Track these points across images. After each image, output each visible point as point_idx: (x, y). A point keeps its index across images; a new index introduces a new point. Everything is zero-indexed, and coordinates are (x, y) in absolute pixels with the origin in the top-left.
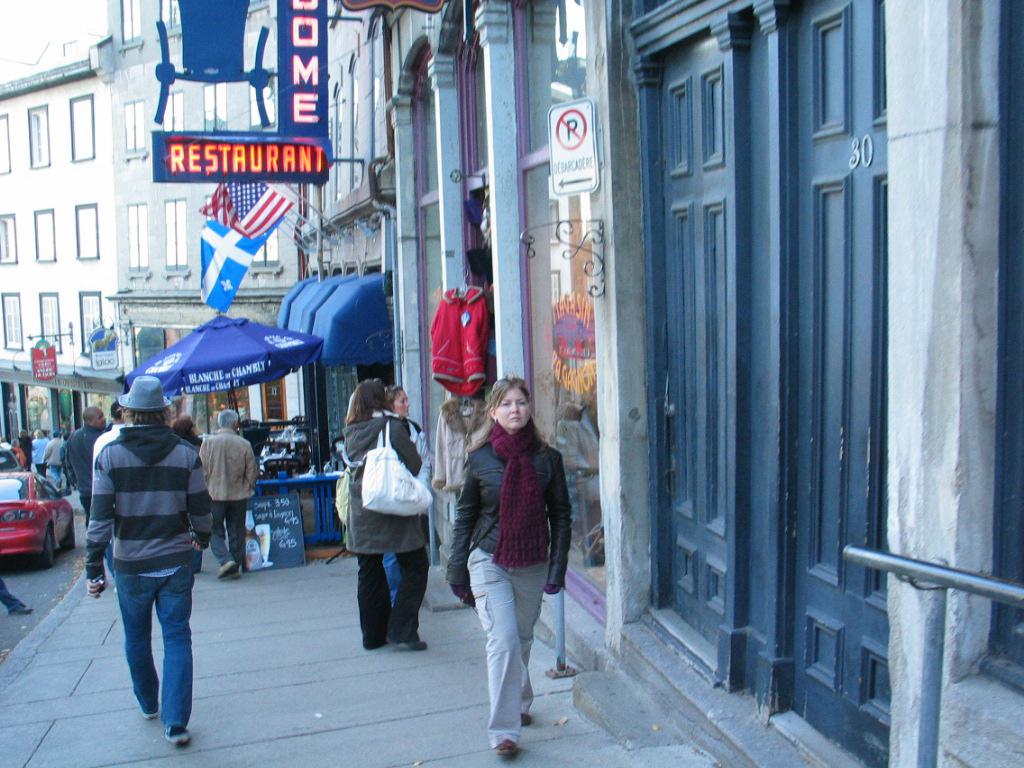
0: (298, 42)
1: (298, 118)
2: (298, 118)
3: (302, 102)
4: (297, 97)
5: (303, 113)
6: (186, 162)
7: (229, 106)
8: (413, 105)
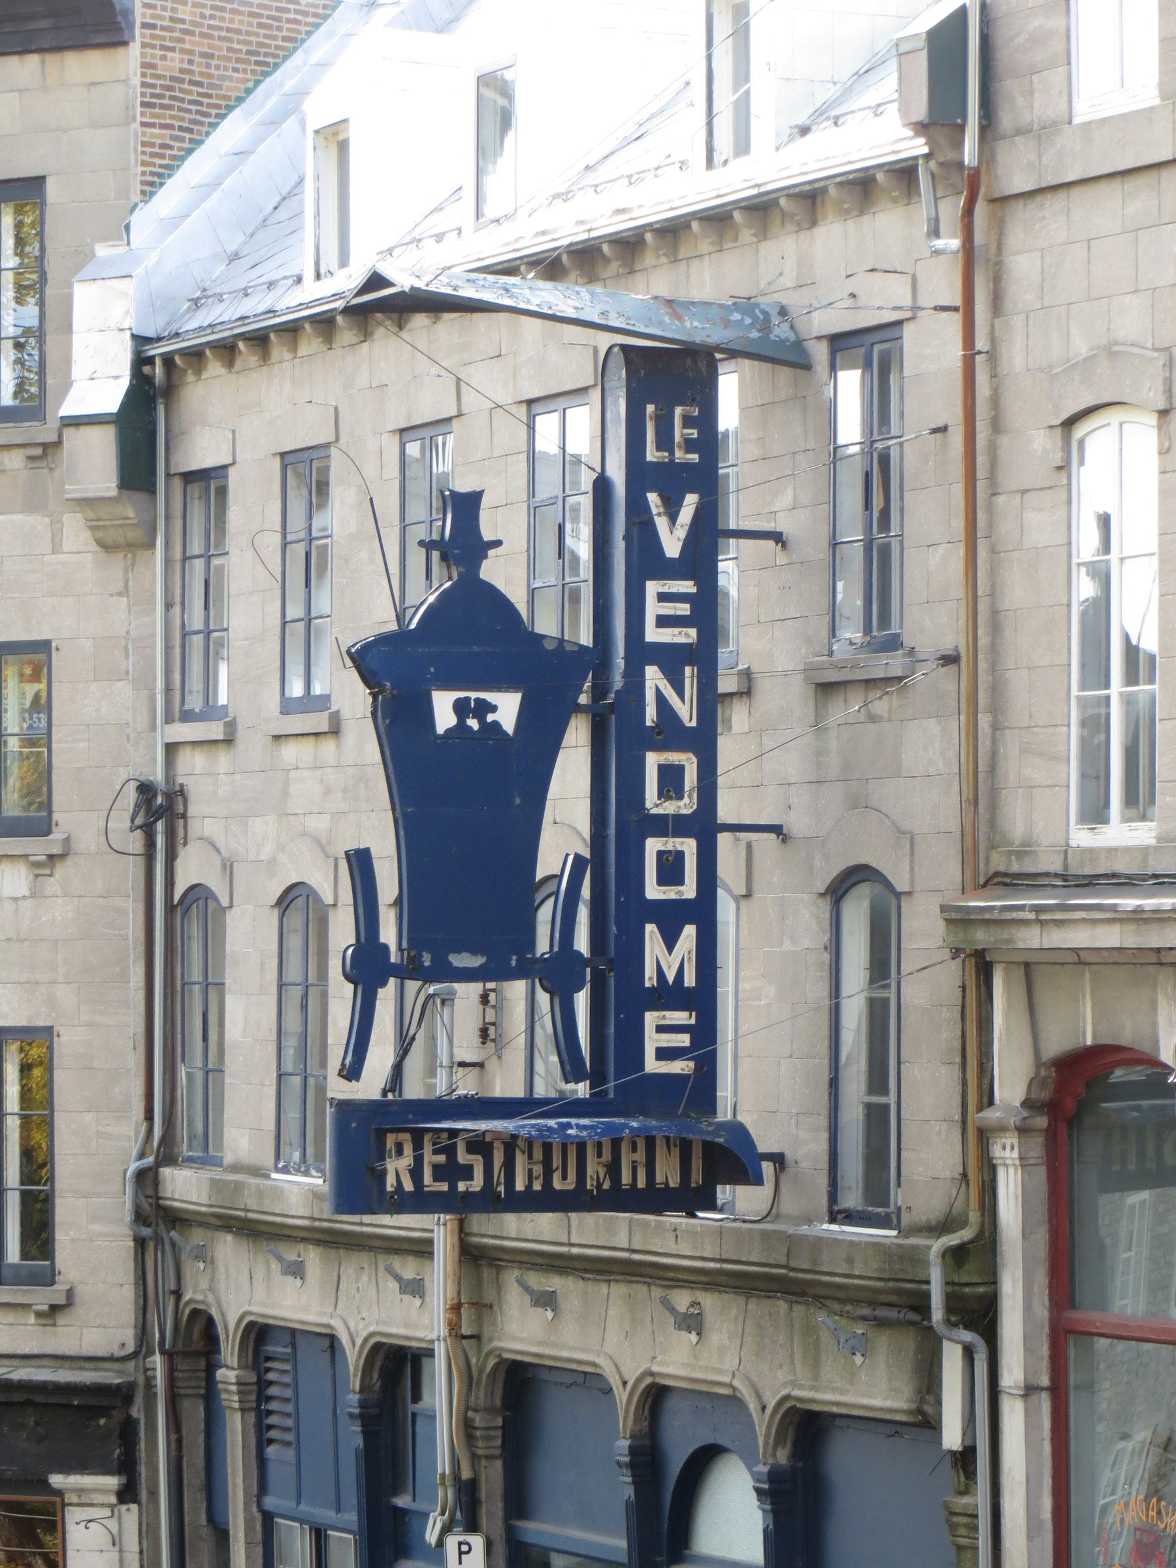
0: (653, 891)
1: (652, 1065)
2: (652, 1065)
3: (661, 1029)
4: (651, 1019)
5: (664, 1054)
6: (416, 1172)
7: (492, 1042)
8: (1051, 1136)
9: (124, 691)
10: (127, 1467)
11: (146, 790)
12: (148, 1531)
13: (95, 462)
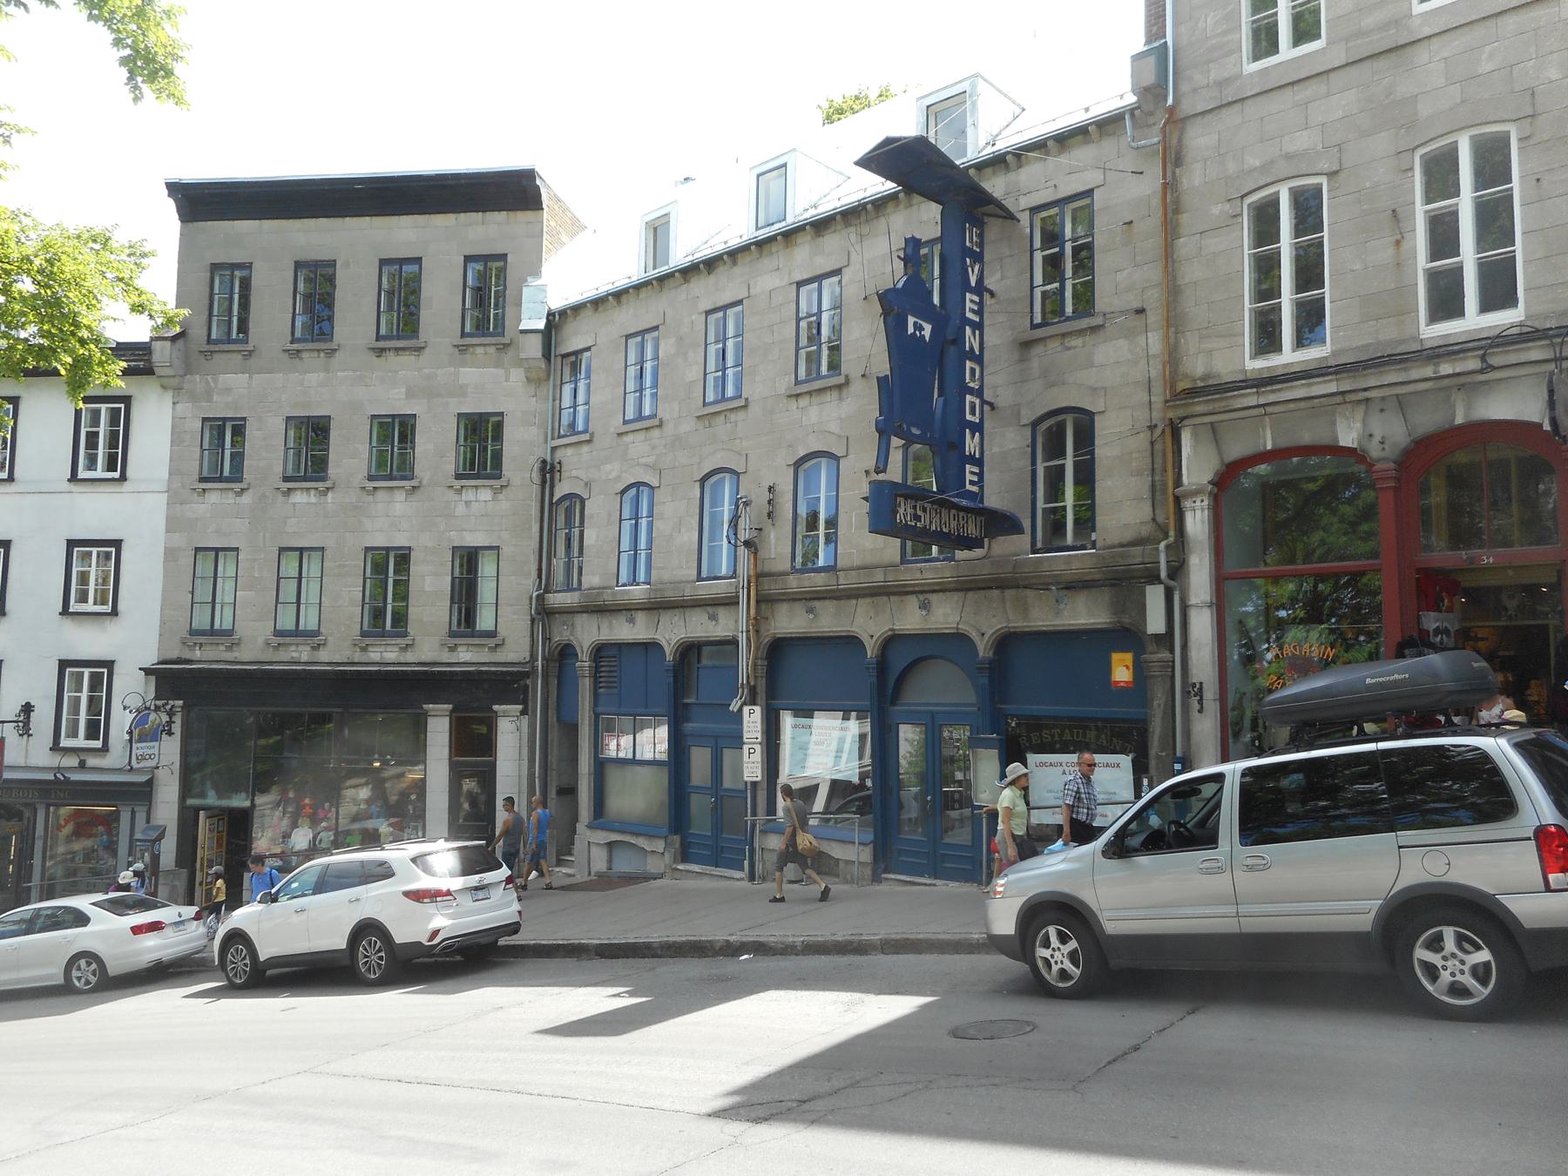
2: (968, 487)
9: (534, 430)
10: (525, 702)
11: (544, 462)
12: (532, 726)
13: (534, 348)
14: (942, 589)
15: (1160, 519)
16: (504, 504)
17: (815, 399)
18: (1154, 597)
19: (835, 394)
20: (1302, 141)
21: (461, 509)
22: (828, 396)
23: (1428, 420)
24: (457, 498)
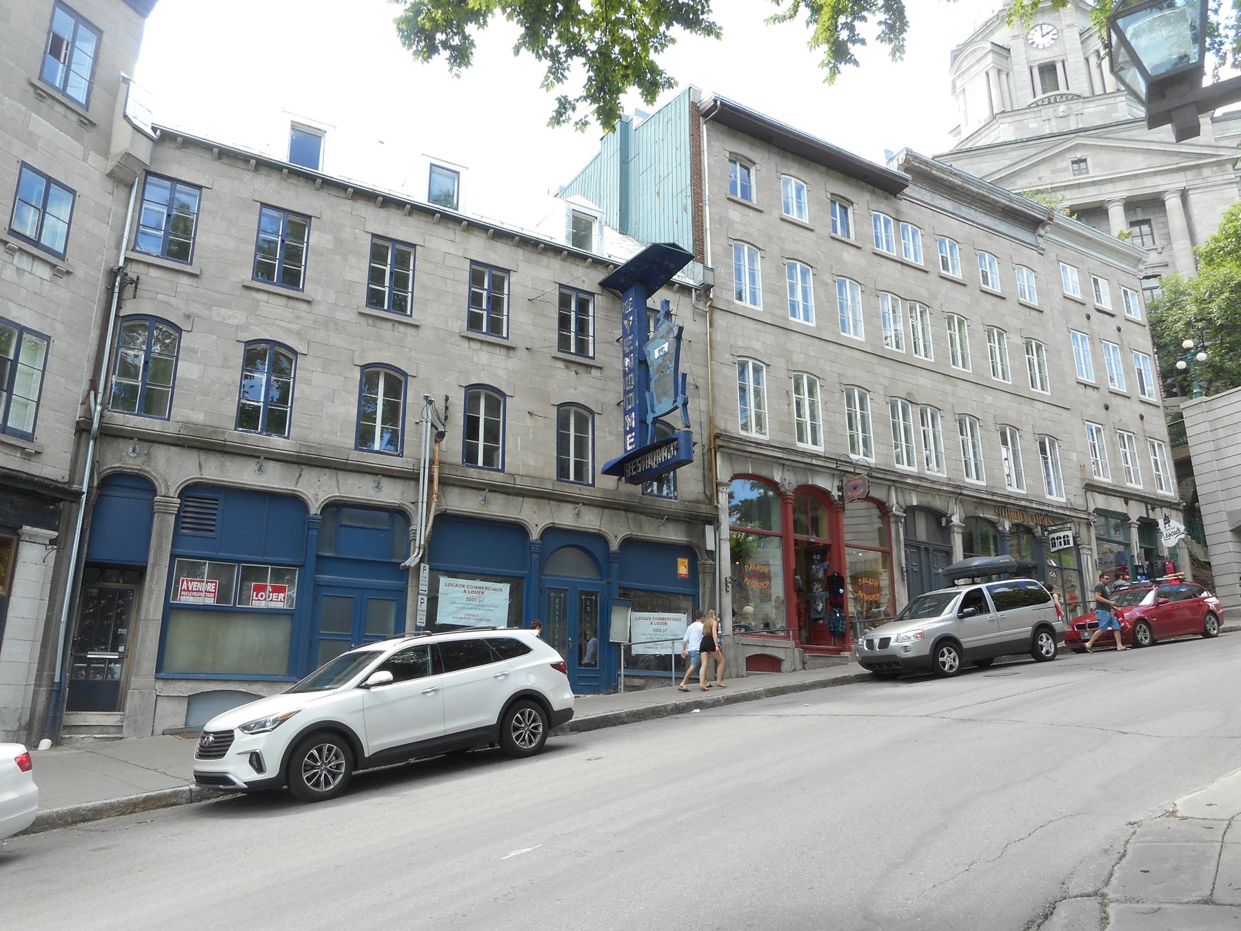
14: (590, 503)
15: (708, 493)
16: (61, 292)
17: (485, 347)
18: (709, 530)
19: (503, 352)
20: (757, 345)
21: (9, 273)
22: (497, 350)
23: (801, 480)
24: (7, 257)
